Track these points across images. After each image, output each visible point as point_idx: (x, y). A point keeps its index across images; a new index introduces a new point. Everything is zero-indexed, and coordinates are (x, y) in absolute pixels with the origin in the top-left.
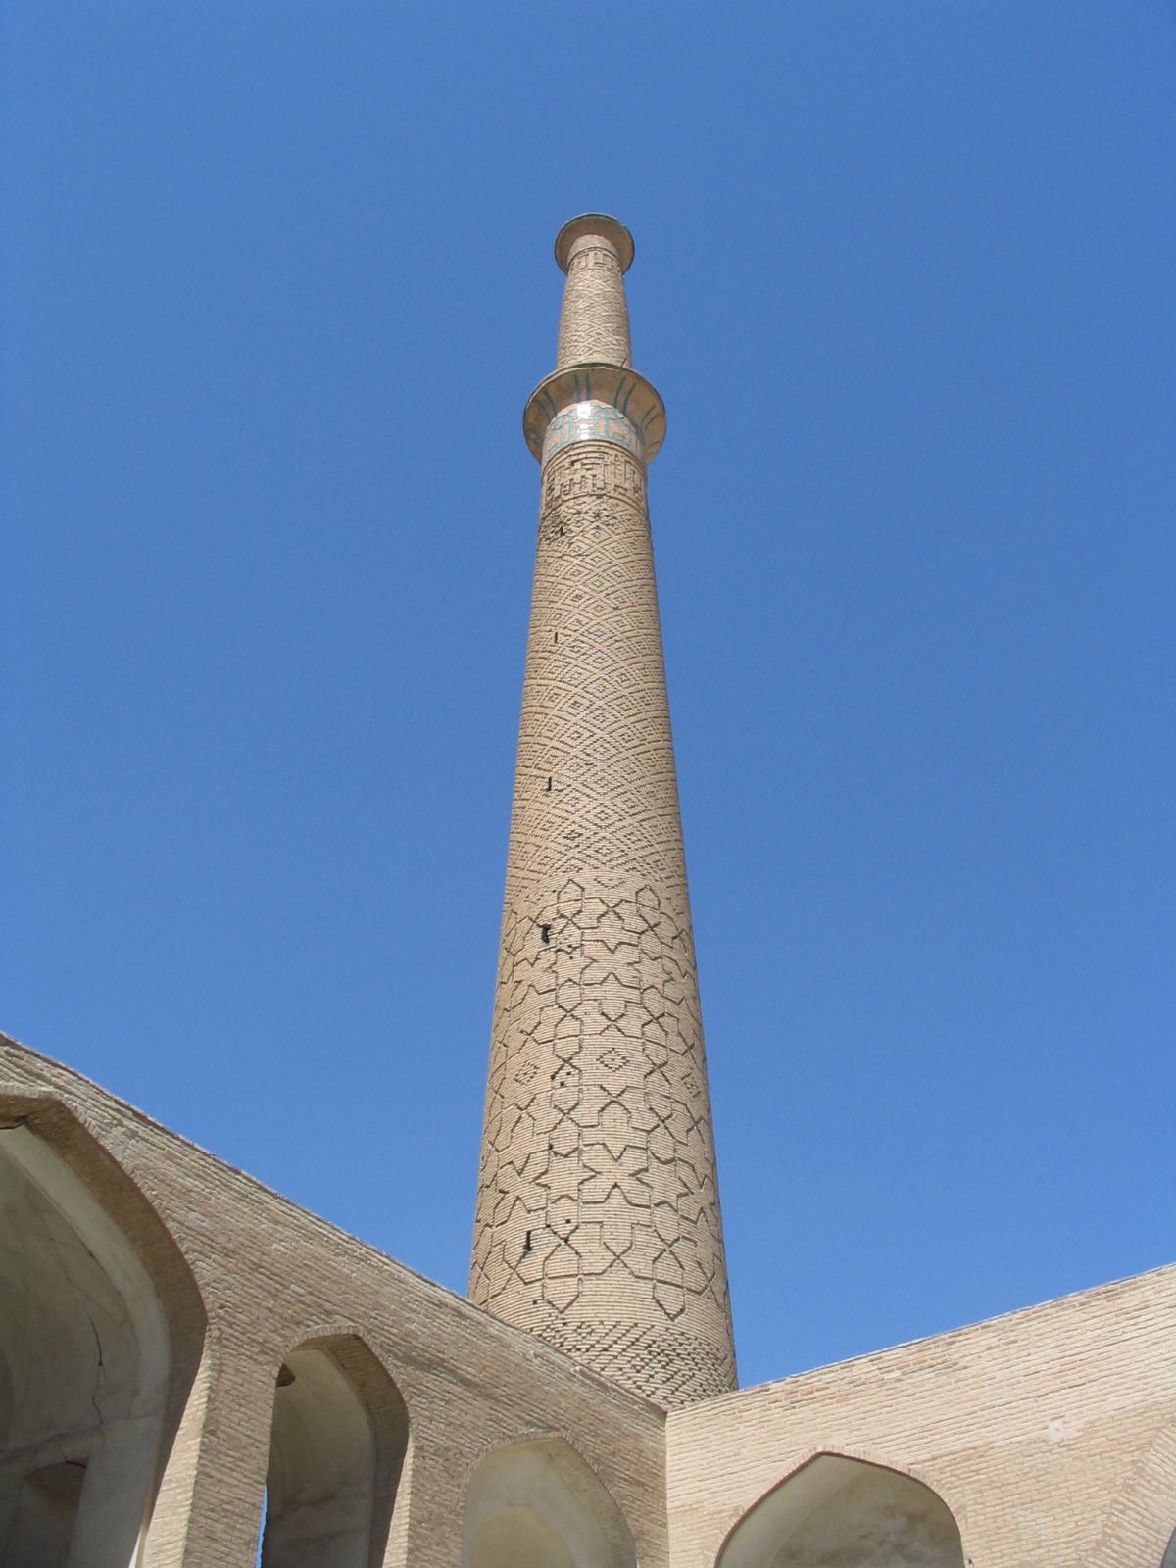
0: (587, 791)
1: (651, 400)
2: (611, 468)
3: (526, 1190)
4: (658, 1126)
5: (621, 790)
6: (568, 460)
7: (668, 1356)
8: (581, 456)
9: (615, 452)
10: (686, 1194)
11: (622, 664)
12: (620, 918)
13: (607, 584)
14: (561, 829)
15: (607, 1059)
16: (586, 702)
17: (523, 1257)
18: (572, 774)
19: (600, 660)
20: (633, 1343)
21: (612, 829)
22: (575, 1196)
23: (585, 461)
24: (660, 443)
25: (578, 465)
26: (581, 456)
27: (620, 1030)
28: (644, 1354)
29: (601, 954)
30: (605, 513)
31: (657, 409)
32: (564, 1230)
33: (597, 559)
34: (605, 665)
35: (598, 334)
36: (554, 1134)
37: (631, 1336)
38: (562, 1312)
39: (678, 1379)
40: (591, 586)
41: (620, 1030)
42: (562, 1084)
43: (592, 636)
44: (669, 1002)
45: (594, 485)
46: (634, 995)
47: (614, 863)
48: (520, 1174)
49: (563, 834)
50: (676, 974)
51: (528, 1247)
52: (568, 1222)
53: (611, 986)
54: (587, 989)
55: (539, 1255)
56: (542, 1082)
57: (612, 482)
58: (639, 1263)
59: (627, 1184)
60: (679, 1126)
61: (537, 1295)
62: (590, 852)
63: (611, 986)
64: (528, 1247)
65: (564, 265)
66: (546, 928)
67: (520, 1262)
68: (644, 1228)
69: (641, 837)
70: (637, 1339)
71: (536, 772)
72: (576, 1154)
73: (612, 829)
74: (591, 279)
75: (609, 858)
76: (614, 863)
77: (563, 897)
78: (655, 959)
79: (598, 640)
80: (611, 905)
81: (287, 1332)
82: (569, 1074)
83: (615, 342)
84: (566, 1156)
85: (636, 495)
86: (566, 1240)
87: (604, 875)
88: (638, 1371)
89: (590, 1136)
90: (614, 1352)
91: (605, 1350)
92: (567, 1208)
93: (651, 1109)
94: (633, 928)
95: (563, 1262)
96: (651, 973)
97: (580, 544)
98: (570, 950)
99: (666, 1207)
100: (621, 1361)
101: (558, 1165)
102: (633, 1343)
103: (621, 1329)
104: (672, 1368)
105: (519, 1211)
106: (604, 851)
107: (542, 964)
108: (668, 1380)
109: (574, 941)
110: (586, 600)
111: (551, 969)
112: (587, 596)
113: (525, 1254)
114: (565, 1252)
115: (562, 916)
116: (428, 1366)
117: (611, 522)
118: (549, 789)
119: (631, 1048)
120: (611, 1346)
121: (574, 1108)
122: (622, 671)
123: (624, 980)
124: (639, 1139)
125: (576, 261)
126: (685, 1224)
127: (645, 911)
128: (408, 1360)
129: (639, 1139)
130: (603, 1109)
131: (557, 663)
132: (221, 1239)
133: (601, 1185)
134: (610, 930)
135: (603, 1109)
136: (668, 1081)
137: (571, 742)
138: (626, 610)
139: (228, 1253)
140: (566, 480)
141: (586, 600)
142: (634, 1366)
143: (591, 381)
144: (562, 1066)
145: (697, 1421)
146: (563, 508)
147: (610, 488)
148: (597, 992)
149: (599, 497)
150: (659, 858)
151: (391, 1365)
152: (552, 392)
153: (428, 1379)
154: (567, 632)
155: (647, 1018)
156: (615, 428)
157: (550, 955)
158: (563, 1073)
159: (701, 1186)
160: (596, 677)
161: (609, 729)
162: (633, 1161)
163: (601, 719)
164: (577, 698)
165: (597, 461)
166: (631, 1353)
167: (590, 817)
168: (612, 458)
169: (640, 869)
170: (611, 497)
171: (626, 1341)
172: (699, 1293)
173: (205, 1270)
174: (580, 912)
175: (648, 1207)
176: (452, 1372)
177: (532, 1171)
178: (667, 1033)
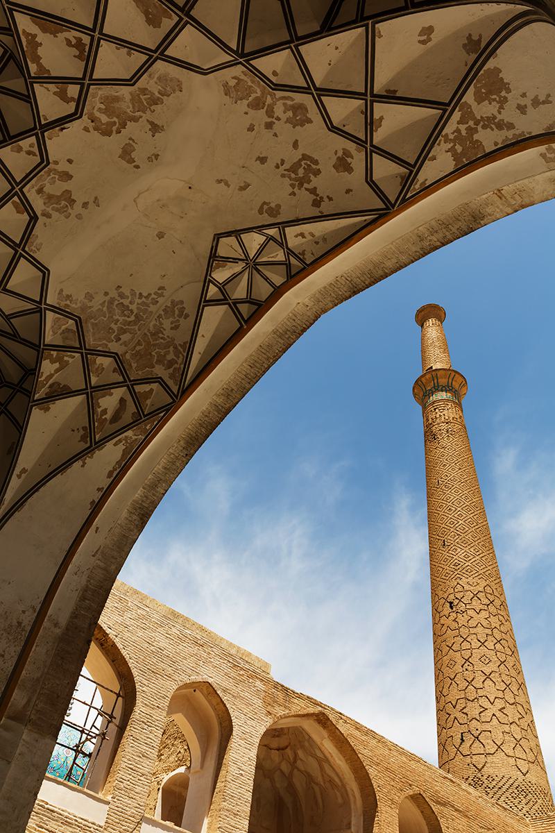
3: (459, 715)
5: (472, 545)
25: (437, 410)
31: (464, 382)
39: (531, 803)
42: (466, 670)
46: (489, 632)
48: (454, 708)
52: (477, 730)
53: (480, 629)
56: (458, 668)
59: (498, 714)
63: (480, 629)
64: (462, 740)
66: (451, 603)
71: (438, 537)
72: (476, 700)
75: (472, 573)
80: (475, 593)
81: (399, 794)
86: (477, 738)
89: (481, 692)
91: (500, 788)
94: (484, 603)
95: (477, 748)
100: (507, 794)
103: (505, 779)
104: (528, 797)
107: (451, 618)
113: (461, 744)
114: (477, 744)
115: (457, 598)
116: (444, 804)
118: (444, 545)
128: (438, 803)
129: (500, 694)
132: (375, 759)
139: (378, 764)
142: (512, 797)
145: (544, 825)
146: (434, 428)
147: (451, 418)
151: (432, 804)
153: (445, 810)
157: (454, 614)
158: (466, 665)
172: (533, 763)
173: (372, 772)
176: (453, 807)
177: (459, 707)
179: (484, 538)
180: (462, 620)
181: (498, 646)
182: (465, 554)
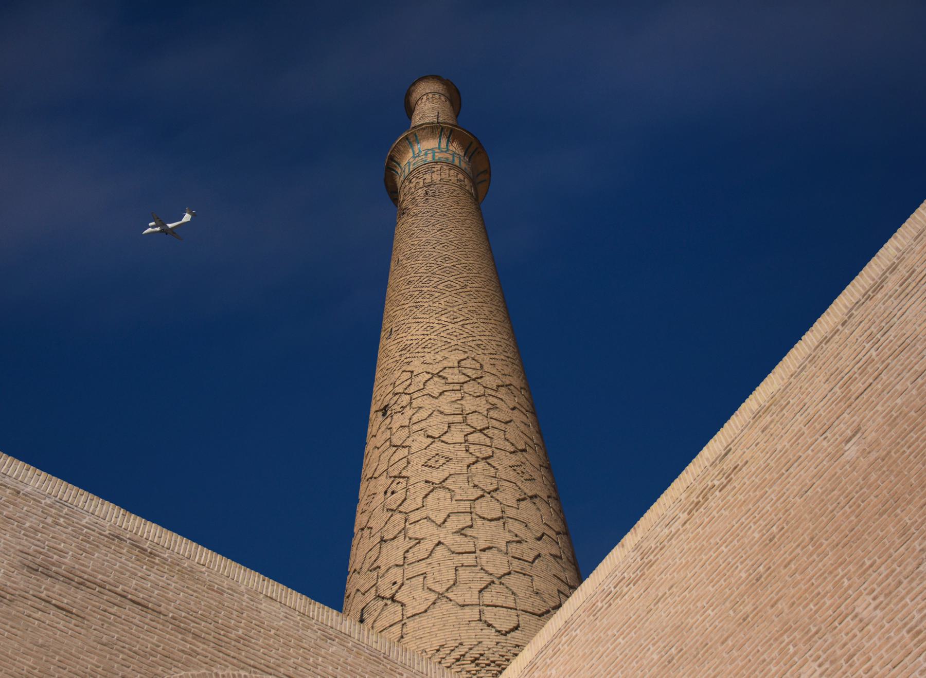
7: (499, 665)
20: (458, 660)
28: (472, 667)
37: (456, 655)
52: (395, 583)
70: (464, 655)
87: (429, 358)
126: (516, 563)
130: (426, 495)
134: (435, 387)
135: (426, 495)
162: (455, 523)
175: (475, 552)
178: (491, 438)
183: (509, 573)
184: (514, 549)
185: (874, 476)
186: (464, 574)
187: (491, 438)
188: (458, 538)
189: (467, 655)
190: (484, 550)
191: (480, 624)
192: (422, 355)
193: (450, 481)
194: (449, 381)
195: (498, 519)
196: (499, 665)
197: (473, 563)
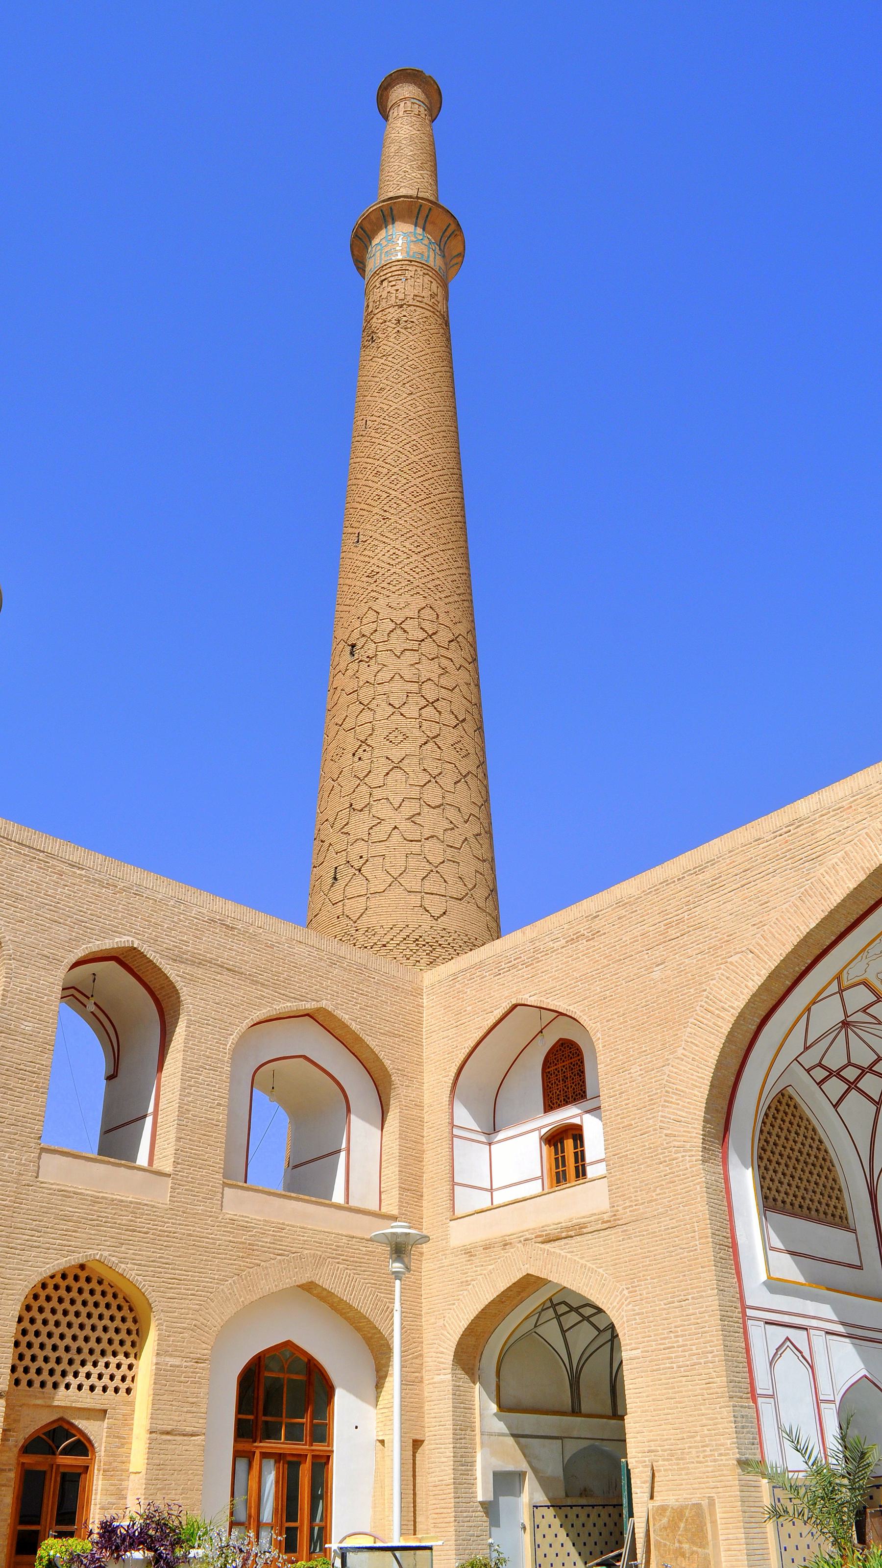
0: (384, 539)
1: (448, 220)
2: (411, 282)
4: (430, 781)
5: (408, 535)
6: (379, 280)
7: (431, 946)
8: (387, 276)
9: (415, 268)
10: (453, 829)
11: (414, 437)
12: (405, 631)
13: (404, 376)
14: (364, 570)
15: (391, 737)
16: (385, 471)
17: (332, 886)
18: (374, 528)
19: (396, 437)
20: (405, 939)
21: (401, 565)
22: (366, 838)
23: (390, 279)
24: (462, 255)
25: (385, 283)
26: (387, 276)
27: (402, 714)
28: (413, 946)
29: (390, 660)
30: (405, 319)
31: (453, 227)
32: (357, 865)
33: (397, 357)
34: (400, 440)
35: (405, 172)
36: (353, 796)
37: (404, 934)
38: (355, 922)
40: (392, 379)
41: (402, 714)
42: (360, 759)
43: (391, 419)
44: (443, 690)
45: (396, 297)
46: (414, 687)
47: (401, 591)
49: (366, 574)
50: (451, 668)
51: (335, 879)
52: (361, 857)
54: (379, 688)
55: (341, 883)
57: (411, 292)
58: (412, 881)
59: (405, 826)
60: (447, 781)
61: (339, 912)
62: (384, 585)
64: (335, 879)
65: (384, 114)
66: (353, 646)
67: (330, 890)
68: (415, 857)
69: (425, 569)
70: (408, 936)
73: (401, 565)
74: (405, 127)
76: (401, 591)
77: (365, 621)
78: (433, 659)
79: (396, 421)
80: (398, 622)
82: (364, 751)
83: (419, 176)
84: (361, 810)
85: (433, 300)
87: (394, 600)
88: (408, 959)
90: (390, 947)
91: (384, 946)
92: (360, 848)
93: (424, 770)
96: (429, 670)
97: (385, 347)
98: (367, 660)
99: (435, 840)
101: (356, 817)
102: (405, 939)
105: (332, 853)
106: (394, 583)
107: (350, 673)
108: (431, 963)
109: (370, 653)
110: (396, 390)
111: (356, 676)
112: (389, 388)
115: (364, 635)
117: (409, 326)
119: (410, 727)
120: (388, 943)
121: (366, 776)
122: (414, 442)
123: (406, 678)
124: (415, 792)
125: (391, 113)
126: (449, 850)
127: (427, 625)
130: (388, 774)
131: (366, 444)
133: (386, 827)
134: (397, 642)
135: (388, 774)
136: (439, 748)
137: (373, 503)
138: (419, 394)
140: (376, 298)
141: (396, 390)
143: (395, 212)
144: (361, 746)
146: (374, 320)
148: (386, 688)
149: (401, 306)
150: (440, 583)
152: (367, 227)
154: (374, 418)
155: (424, 703)
156: (415, 248)
157: (355, 666)
159: (466, 822)
160: (393, 450)
161: (401, 490)
162: (409, 809)
163: (395, 482)
164: (380, 469)
165: (400, 277)
166: (403, 946)
167: (385, 558)
168: (412, 274)
169: (422, 593)
170: (409, 305)
171: (399, 938)
174: (376, 631)
175: (420, 841)
178: (440, 713)
179: (440, 522)
180: (366, 673)
181: (429, 712)
182: (392, 552)
183: (444, 862)
184: (449, 837)
185: (661, 1000)
186: (413, 862)
187: (440, 713)
188: (410, 824)
189: (411, 936)
190: (427, 839)
191: (421, 909)
192: (388, 593)
193: (405, 762)
194: (410, 637)
195: (439, 806)
196: (431, 946)
197: (418, 851)
